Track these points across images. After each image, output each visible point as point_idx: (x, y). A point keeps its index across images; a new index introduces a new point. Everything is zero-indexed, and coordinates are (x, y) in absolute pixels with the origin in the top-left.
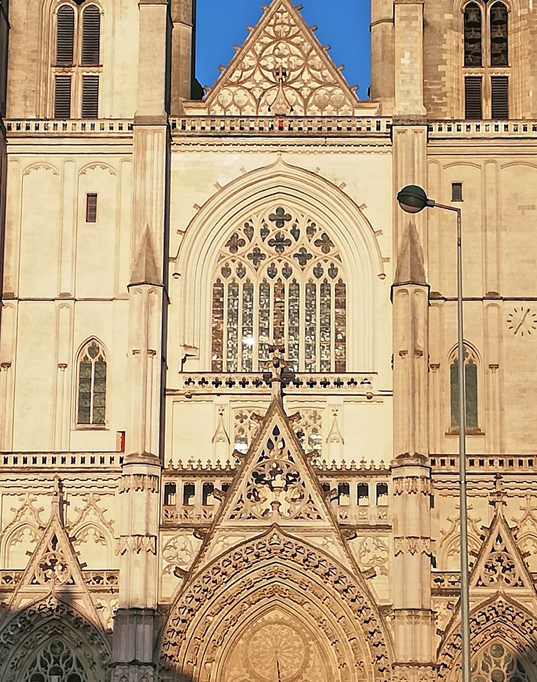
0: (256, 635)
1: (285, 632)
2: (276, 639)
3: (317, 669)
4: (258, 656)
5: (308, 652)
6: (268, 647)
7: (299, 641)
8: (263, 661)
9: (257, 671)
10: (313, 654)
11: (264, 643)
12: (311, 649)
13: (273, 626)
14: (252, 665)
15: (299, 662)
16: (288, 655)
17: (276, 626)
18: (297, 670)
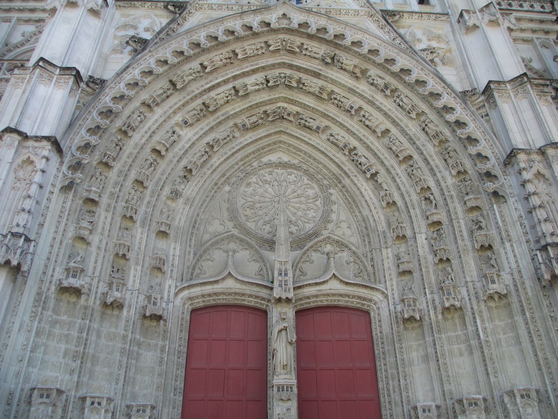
0: (250, 181)
1: (292, 178)
2: (280, 185)
3: (344, 225)
4: (251, 207)
5: (328, 201)
6: (267, 195)
7: (312, 188)
8: (260, 212)
9: (251, 225)
10: (336, 206)
11: (261, 191)
12: (333, 198)
13: (276, 170)
14: (243, 218)
15: (314, 214)
16: (298, 205)
17: (279, 171)
18: (312, 225)
